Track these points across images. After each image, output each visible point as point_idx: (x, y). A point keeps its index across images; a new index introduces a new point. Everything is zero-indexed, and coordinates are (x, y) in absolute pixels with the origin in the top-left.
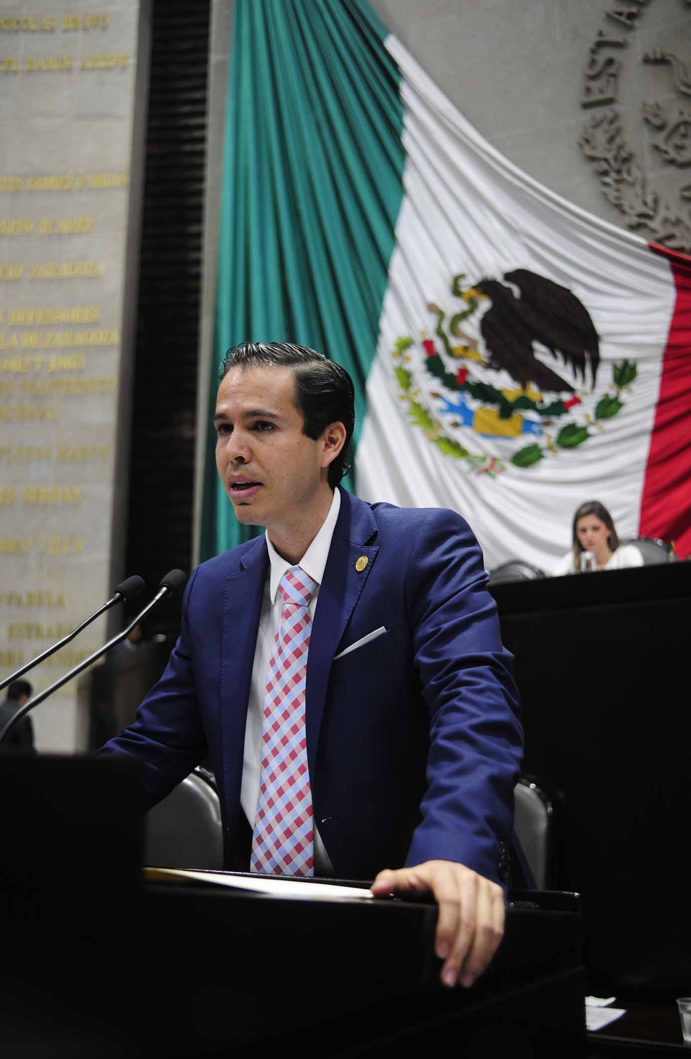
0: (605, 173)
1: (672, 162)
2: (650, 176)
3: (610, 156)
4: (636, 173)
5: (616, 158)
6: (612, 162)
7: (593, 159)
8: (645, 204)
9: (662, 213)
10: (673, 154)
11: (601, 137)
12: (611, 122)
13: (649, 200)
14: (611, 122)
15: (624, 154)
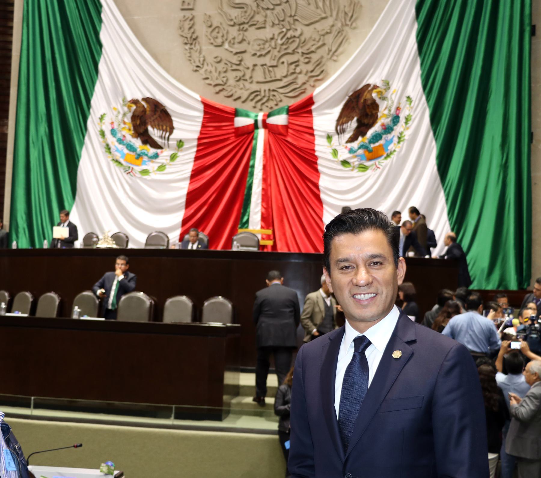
0: (186, 44)
1: (212, 44)
2: (204, 48)
3: (189, 36)
4: (198, 47)
5: (191, 37)
6: (189, 39)
7: (182, 36)
8: (199, 61)
9: (205, 67)
10: (212, 41)
11: (187, 25)
12: (191, 20)
13: (202, 59)
14: (191, 20)
15: (194, 37)
